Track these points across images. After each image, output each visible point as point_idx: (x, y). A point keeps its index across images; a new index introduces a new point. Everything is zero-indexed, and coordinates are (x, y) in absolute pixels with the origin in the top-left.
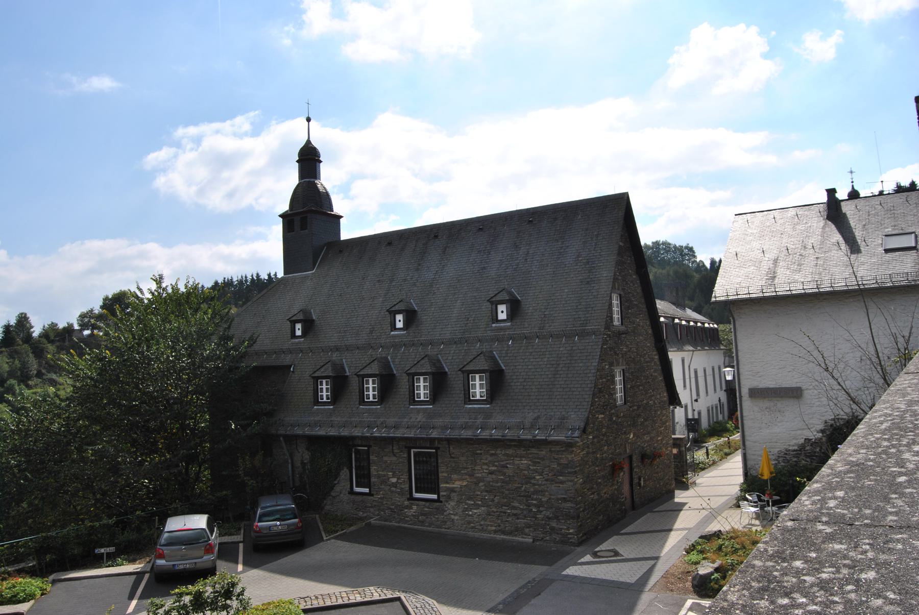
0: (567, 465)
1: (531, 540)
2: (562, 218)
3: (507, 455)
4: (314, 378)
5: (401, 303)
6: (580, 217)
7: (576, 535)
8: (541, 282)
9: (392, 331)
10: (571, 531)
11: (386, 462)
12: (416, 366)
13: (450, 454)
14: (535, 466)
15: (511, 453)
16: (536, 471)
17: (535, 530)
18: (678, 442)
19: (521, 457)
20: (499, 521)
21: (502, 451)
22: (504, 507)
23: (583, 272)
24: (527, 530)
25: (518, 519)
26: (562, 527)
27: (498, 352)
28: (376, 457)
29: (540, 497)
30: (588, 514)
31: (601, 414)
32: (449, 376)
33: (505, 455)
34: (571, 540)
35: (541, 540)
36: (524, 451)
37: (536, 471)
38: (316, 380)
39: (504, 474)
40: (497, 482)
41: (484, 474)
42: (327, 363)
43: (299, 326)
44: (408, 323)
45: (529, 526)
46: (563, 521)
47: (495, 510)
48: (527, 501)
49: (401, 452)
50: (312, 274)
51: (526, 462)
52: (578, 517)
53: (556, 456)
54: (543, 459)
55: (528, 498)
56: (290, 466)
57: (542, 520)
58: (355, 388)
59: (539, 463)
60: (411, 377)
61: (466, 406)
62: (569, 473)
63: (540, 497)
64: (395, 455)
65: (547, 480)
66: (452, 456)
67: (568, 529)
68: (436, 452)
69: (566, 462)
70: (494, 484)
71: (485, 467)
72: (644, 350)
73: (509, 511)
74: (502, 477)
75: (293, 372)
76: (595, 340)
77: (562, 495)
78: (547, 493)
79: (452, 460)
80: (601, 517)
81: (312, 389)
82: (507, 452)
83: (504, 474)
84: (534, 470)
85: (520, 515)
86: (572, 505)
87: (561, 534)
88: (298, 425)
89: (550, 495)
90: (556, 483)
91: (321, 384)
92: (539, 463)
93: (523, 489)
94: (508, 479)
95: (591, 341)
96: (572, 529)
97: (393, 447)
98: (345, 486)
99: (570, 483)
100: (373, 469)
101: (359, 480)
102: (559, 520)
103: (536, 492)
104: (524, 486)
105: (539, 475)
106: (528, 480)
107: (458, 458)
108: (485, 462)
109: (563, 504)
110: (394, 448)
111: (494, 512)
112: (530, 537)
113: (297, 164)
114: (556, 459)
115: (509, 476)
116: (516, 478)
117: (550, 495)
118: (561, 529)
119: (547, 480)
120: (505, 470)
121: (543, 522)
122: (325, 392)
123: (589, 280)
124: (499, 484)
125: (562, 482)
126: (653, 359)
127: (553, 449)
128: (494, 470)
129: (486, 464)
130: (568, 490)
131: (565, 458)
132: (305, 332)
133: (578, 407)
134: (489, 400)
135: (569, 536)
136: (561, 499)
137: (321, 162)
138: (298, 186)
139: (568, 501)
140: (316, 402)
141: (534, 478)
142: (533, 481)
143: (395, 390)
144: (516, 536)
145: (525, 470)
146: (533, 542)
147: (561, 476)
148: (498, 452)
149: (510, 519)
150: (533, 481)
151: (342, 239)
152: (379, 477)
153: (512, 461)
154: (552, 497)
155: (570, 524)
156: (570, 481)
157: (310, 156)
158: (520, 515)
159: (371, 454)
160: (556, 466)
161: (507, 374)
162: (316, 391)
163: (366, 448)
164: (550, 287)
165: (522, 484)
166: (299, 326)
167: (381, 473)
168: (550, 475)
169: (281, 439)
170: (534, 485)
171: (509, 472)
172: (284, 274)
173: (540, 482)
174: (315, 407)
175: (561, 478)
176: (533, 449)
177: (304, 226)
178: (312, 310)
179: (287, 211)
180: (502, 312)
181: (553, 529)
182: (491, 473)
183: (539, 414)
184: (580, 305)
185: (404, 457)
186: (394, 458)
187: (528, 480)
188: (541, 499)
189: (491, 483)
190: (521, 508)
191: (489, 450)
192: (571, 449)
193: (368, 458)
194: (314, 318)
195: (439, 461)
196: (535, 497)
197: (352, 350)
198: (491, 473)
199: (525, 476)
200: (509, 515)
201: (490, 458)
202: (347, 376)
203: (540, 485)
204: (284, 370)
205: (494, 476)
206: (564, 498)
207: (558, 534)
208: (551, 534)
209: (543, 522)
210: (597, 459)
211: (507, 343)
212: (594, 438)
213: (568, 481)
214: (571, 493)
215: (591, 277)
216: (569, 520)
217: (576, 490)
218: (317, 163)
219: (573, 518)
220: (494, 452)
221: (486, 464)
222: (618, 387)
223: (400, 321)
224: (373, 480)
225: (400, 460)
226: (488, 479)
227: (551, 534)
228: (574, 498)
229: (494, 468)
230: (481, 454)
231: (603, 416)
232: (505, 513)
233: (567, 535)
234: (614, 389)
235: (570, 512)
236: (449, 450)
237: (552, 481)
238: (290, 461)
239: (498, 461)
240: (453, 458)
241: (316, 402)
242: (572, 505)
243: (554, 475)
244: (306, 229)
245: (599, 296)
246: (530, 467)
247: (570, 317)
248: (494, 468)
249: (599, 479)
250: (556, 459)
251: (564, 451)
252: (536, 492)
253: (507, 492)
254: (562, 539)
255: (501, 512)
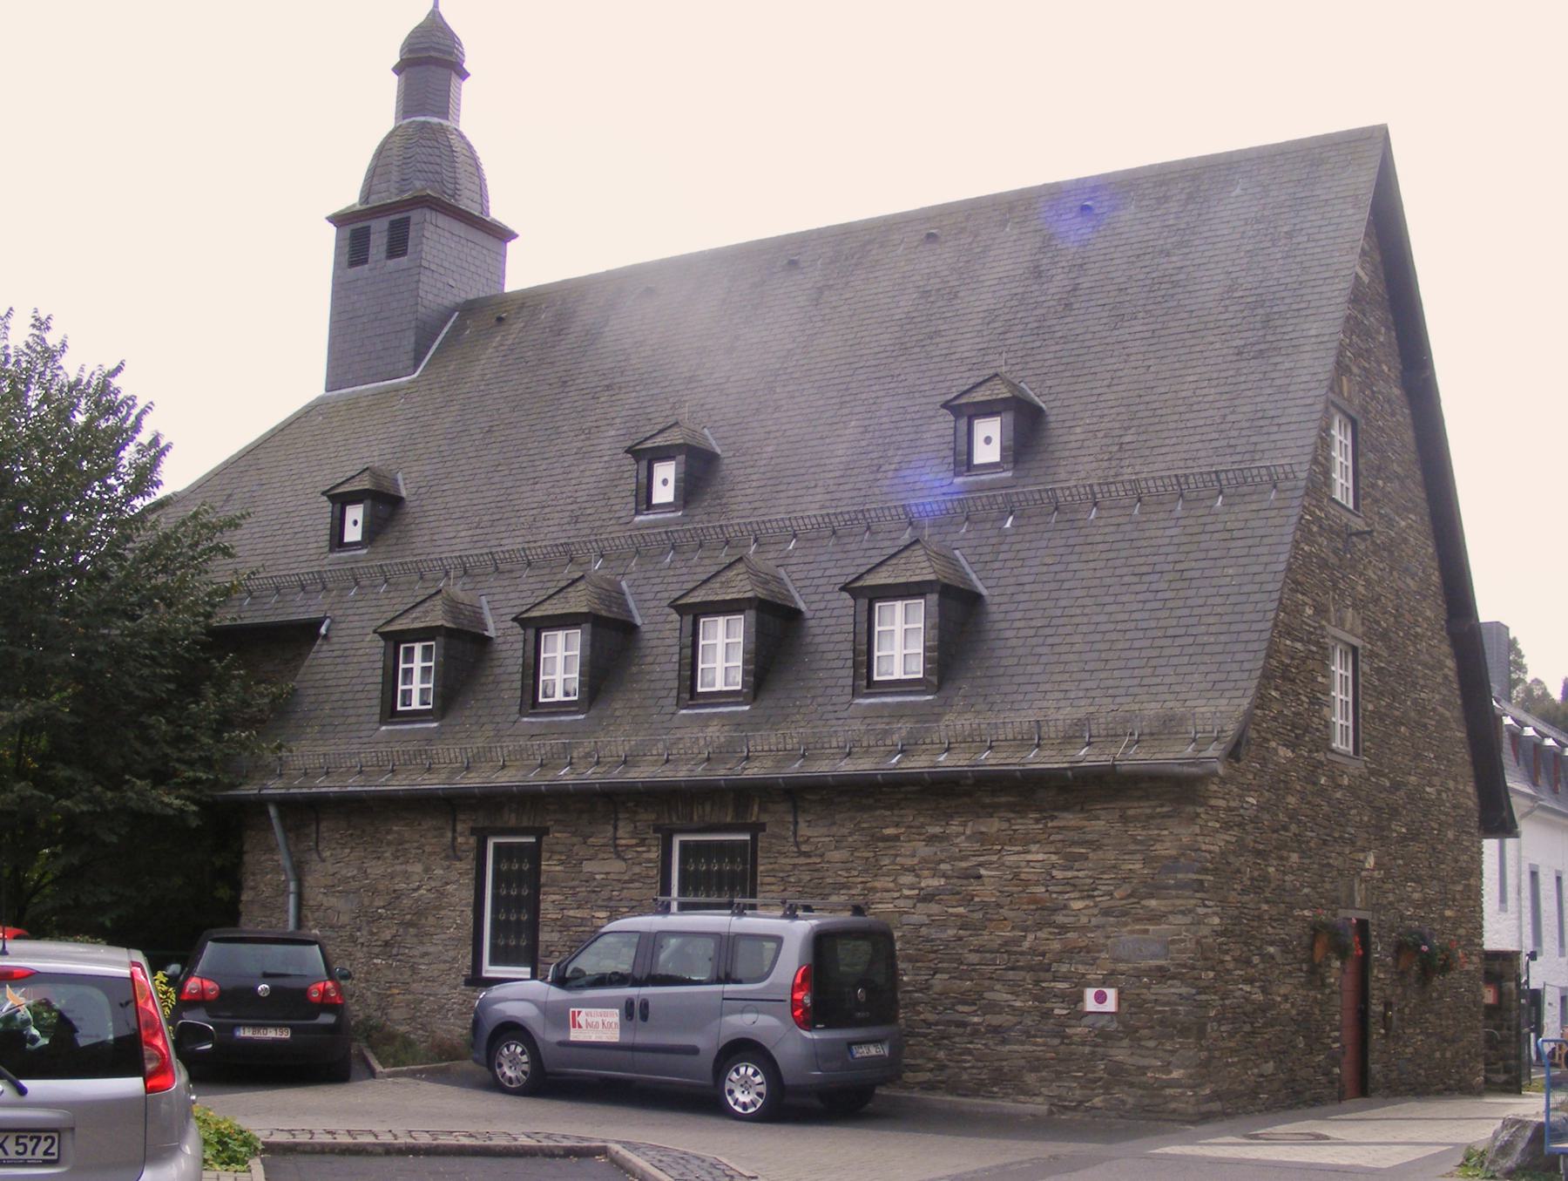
0: (1176, 859)
1: (1045, 1107)
2: (1183, 196)
3: (982, 838)
4: (385, 636)
5: (675, 429)
6: (1238, 191)
7: (1191, 1087)
8: (1113, 360)
9: (638, 513)
10: (1176, 1074)
11: (591, 878)
12: (709, 585)
13: (797, 844)
14: (1071, 868)
15: (994, 829)
16: (1071, 884)
17: (1059, 1075)
18: (1496, 966)
19: (1027, 841)
20: (941, 1055)
21: (964, 824)
22: (960, 1008)
23: (1246, 327)
24: (1031, 1078)
25: (1004, 1042)
26: (1146, 1062)
27: (967, 551)
28: (562, 863)
29: (1082, 969)
30: (1231, 1035)
31: (1287, 747)
32: (812, 623)
33: (982, 838)
34: (1173, 1105)
35: (1074, 1109)
36: (1037, 821)
37: (1071, 884)
38: (396, 640)
39: (968, 900)
40: (943, 926)
41: (901, 903)
42: (430, 597)
43: (355, 513)
44: (689, 491)
45: (1035, 1065)
46: (1152, 1044)
47: (932, 1017)
48: (1037, 982)
49: (642, 842)
50: (413, 381)
51: (1040, 857)
52: (1202, 1033)
53: (1141, 834)
54: (1095, 845)
55: (1042, 975)
56: (292, 899)
57: (1083, 1044)
58: (510, 669)
59: (1085, 857)
60: (690, 618)
61: (857, 701)
62: (1181, 886)
63: (1082, 969)
64: (619, 856)
65: (1106, 912)
66: (804, 848)
67: (1167, 1068)
68: (754, 839)
69: (1173, 852)
70: (934, 933)
71: (907, 879)
72: (1416, 624)
73: (976, 1019)
74: (961, 910)
75: (326, 637)
76: (1277, 504)
77: (1154, 956)
78: (1104, 955)
79: (802, 860)
80: (1269, 1067)
81: (380, 679)
82: (983, 829)
83: (968, 900)
84: (1067, 882)
85: (1010, 1029)
86: (1184, 990)
87: (1143, 1086)
88: (327, 773)
89: (1116, 960)
90: (1138, 920)
91: (409, 653)
92: (1085, 857)
93: (1026, 945)
94: (979, 915)
95: (1265, 505)
96: (1179, 1067)
97: (616, 828)
98: (455, 959)
99: (1180, 919)
100: (549, 904)
101: (504, 867)
102: (1140, 1039)
103: (1069, 952)
104: (1031, 937)
105: (1082, 898)
106: (1045, 912)
107: (822, 856)
108: (909, 862)
109: (1155, 989)
110: (620, 833)
111: (929, 1025)
112: (1040, 1099)
113: (395, 78)
114: (1140, 842)
115: (984, 905)
116: (1005, 912)
117: (1116, 960)
118: (1143, 1070)
119: (1106, 912)
120: (974, 887)
121: (1087, 1049)
122: (417, 688)
123: (1263, 346)
124: (951, 932)
125: (1156, 918)
126: (1442, 666)
127: (1131, 812)
128: (937, 888)
129: (912, 870)
130: (1173, 942)
131: (1173, 838)
132: (373, 531)
133: (1218, 686)
134: (934, 679)
135: (1169, 1091)
136: (1149, 972)
137: (464, 75)
138: (391, 134)
139: (1173, 978)
140: (390, 714)
141: (1065, 907)
142: (1060, 918)
143: (634, 669)
144: (992, 1096)
145: (1037, 883)
146: (1051, 1113)
147: (1151, 896)
148: (954, 828)
149: (978, 1045)
150: (1060, 918)
151: (509, 288)
152: (564, 925)
153: (995, 858)
154: (1122, 967)
155: (1173, 1052)
156: (1183, 913)
157: (433, 54)
158: (1010, 1029)
159: (545, 855)
160: (1138, 866)
161: (994, 609)
162: (390, 678)
163: (532, 840)
164: (1142, 370)
165: (1026, 929)
166: (355, 513)
167: (571, 913)
168: (1116, 895)
169: (272, 811)
170: (1064, 929)
171: (986, 892)
172: (327, 390)
173: (1084, 920)
174: (384, 728)
175: (1153, 903)
176: (1066, 815)
177: (398, 244)
178: (400, 476)
179: (354, 205)
180: (988, 440)
181: (1117, 1073)
182: (927, 898)
183: (1092, 709)
184: (1233, 413)
185: (649, 861)
186: (617, 866)
187: (1045, 912)
188: (1084, 975)
189: (924, 931)
190: (1014, 1008)
191: (922, 826)
192: (1189, 809)
193: (536, 870)
194: (404, 493)
195: (761, 868)
196: (1064, 968)
197: (511, 571)
198: (927, 898)
199: (1035, 901)
200: (975, 1033)
201: (924, 850)
202: (490, 639)
203: (1083, 929)
204: (304, 634)
205: (934, 908)
206: (1160, 969)
207: (1131, 1085)
208: (1107, 1089)
209: (1087, 1049)
210: (1265, 878)
211: (997, 524)
212: (1260, 808)
213: (1171, 912)
214: (1180, 951)
215: (1269, 338)
216: (1171, 1037)
217: (1198, 942)
218: (454, 79)
219: (1184, 1031)
220: (937, 830)
221: (912, 870)
222: (1338, 695)
223: (665, 482)
224: (544, 936)
225: (637, 869)
226: (915, 919)
227: (1107, 1089)
228: (1193, 968)
229: (935, 882)
230: (896, 838)
231: (1290, 754)
232: (964, 1024)
233: (1163, 1088)
234: (1328, 725)
235: (1175, 1012)
236: (795, 834)
237: (1124, 914)
238: (292, 886)
239: (952, 859)
240: (807, 855)
241: (390, 714)
242: (1184, 990)
243: (1129, 896)
244: (404, 253)
245: (1292, 388)
246: (1055, 873)
247: (1199, 445)
248: (935, 882)
249: (1272, 943)
250: (1140, 842)
251: (1164, 816)
252: (1069, 952)
253: (974, 958)
254: (1146, 1101)
255: (949, 1023)
